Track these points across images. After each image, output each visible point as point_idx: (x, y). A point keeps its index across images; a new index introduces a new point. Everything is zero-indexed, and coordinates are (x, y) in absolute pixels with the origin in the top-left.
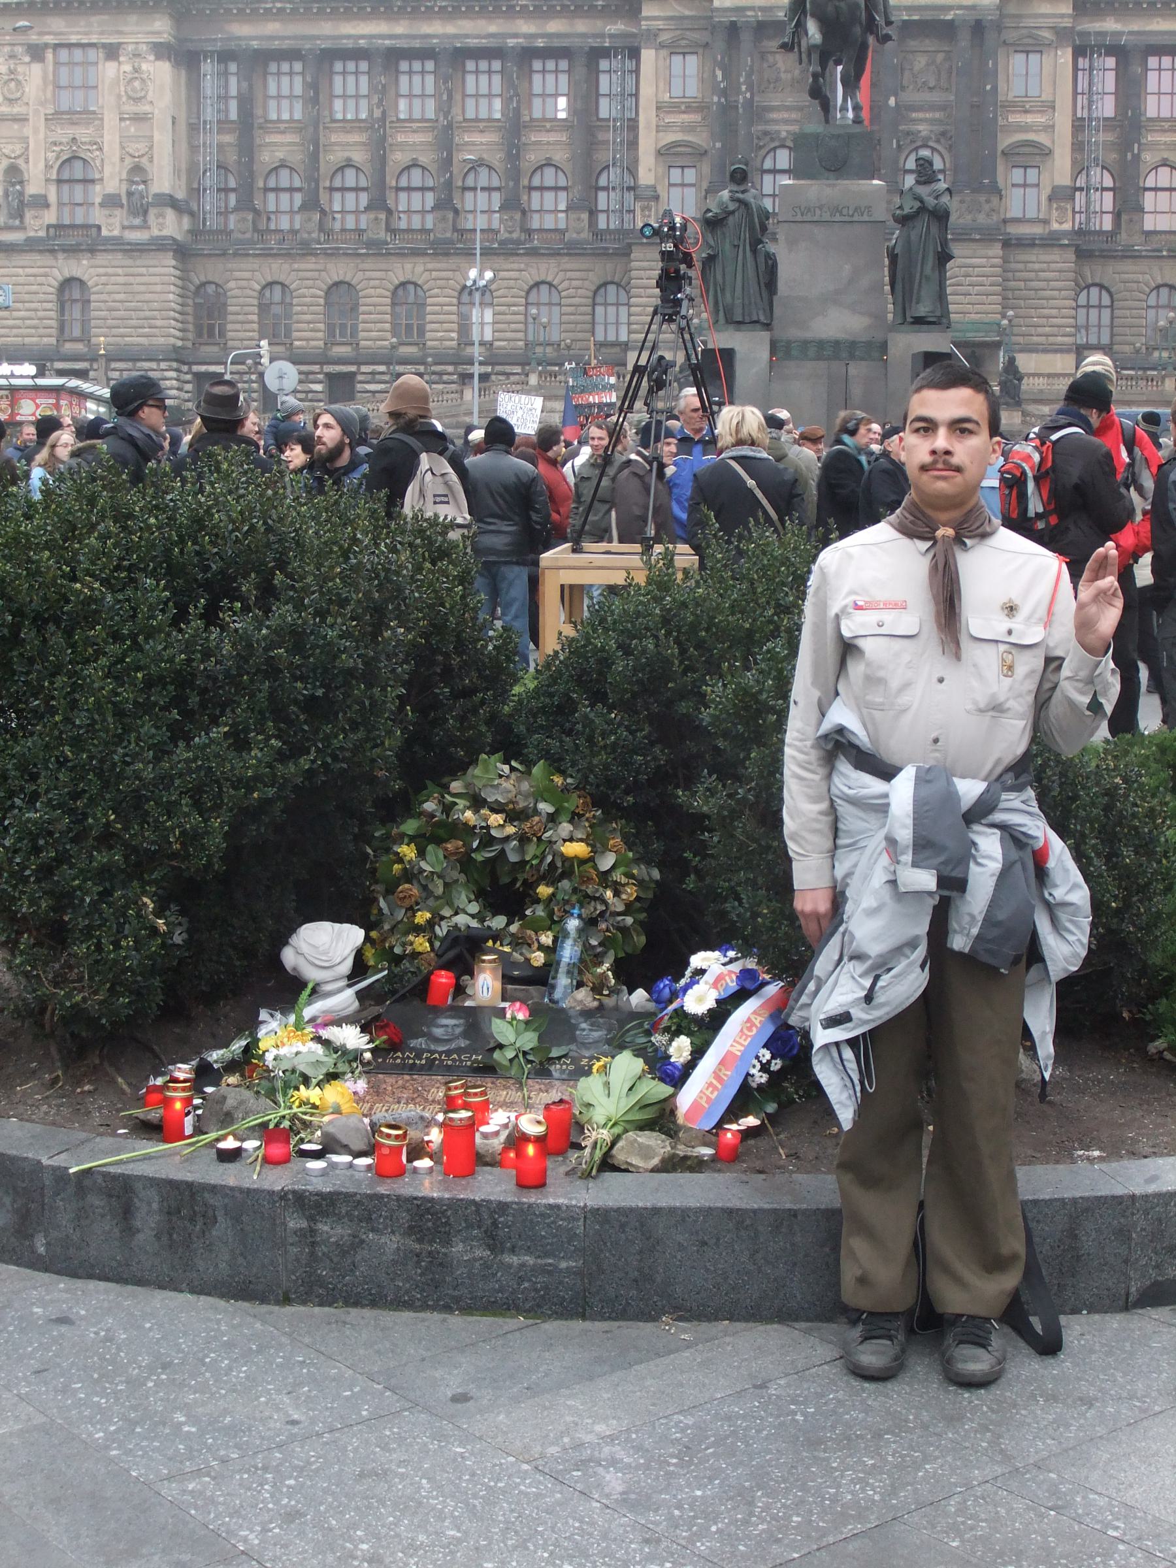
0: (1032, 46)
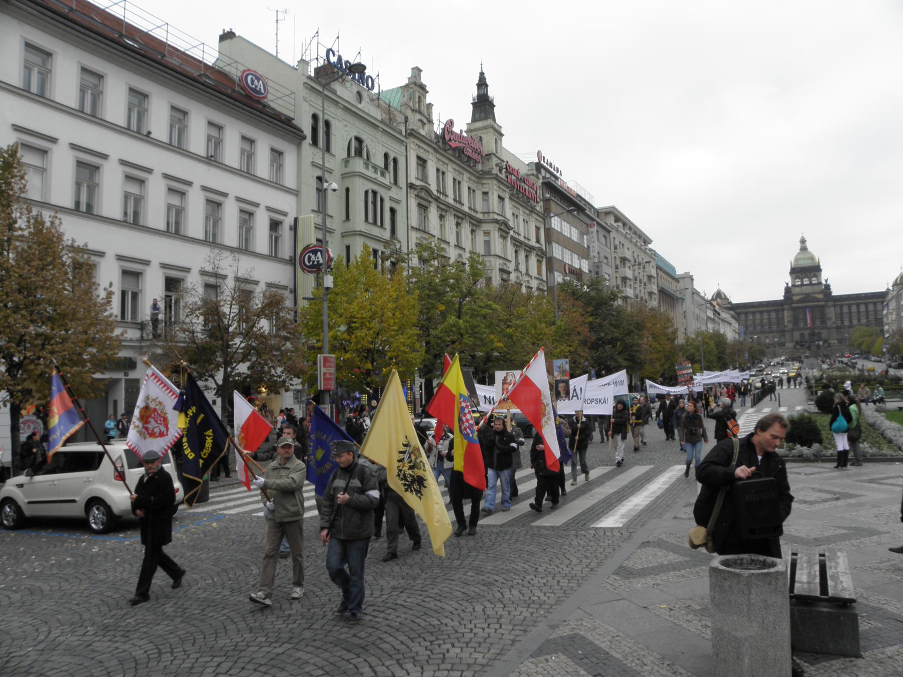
0: (829, 307)
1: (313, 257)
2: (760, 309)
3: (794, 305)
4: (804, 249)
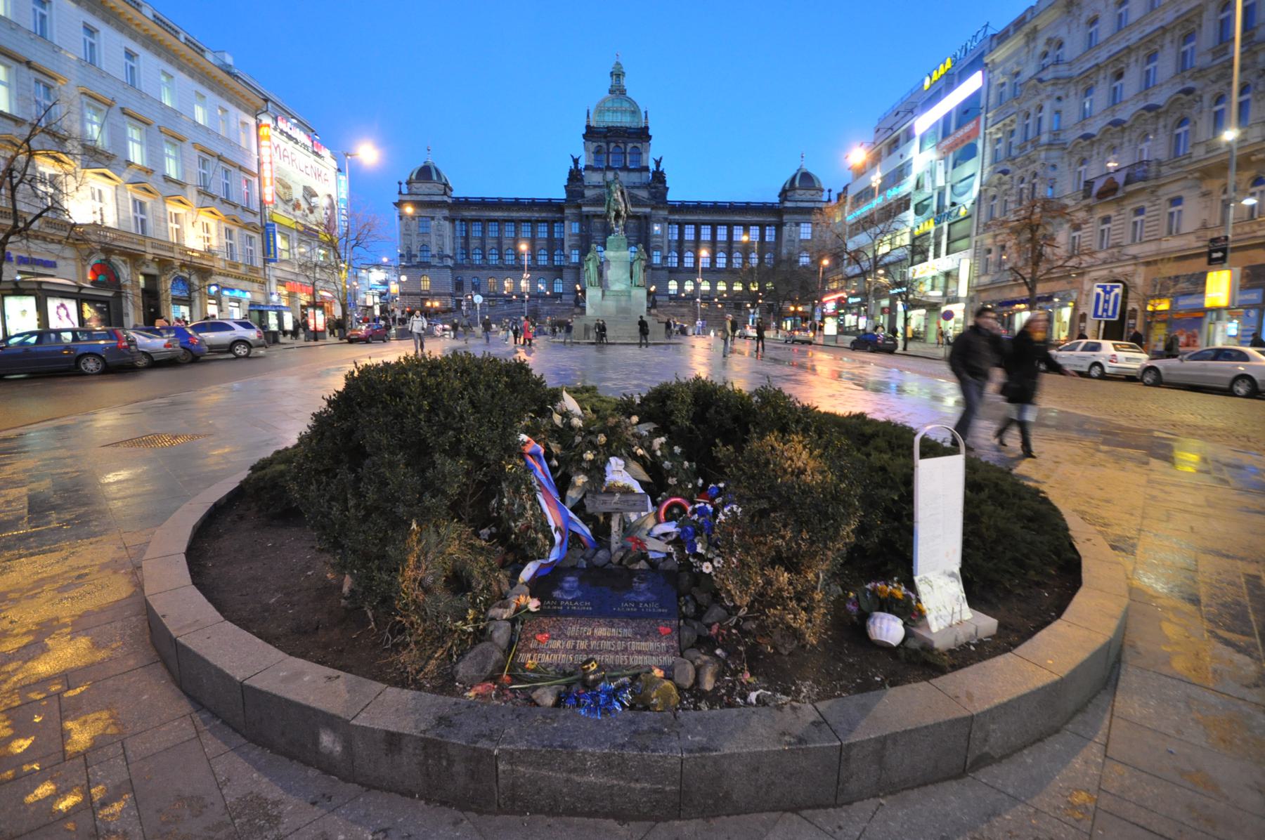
2: (515, 215)
3: (585, 209)
4: (618, 91)
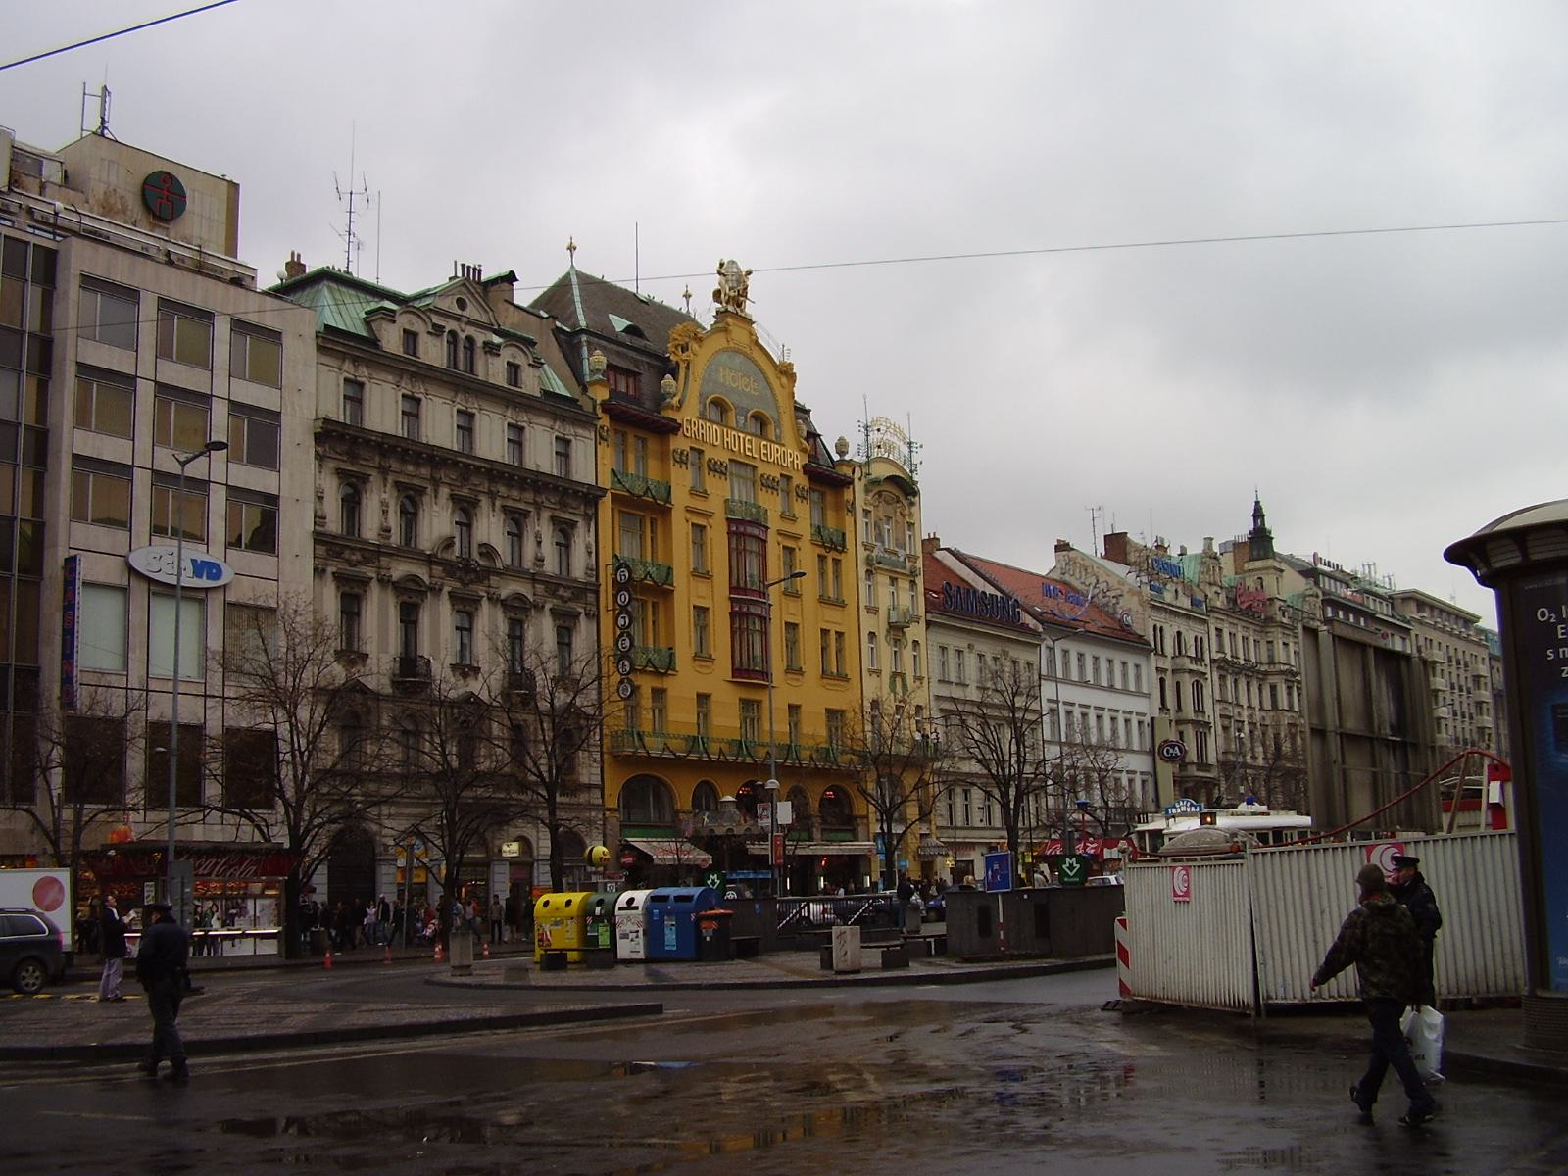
1: (1171, 751)
